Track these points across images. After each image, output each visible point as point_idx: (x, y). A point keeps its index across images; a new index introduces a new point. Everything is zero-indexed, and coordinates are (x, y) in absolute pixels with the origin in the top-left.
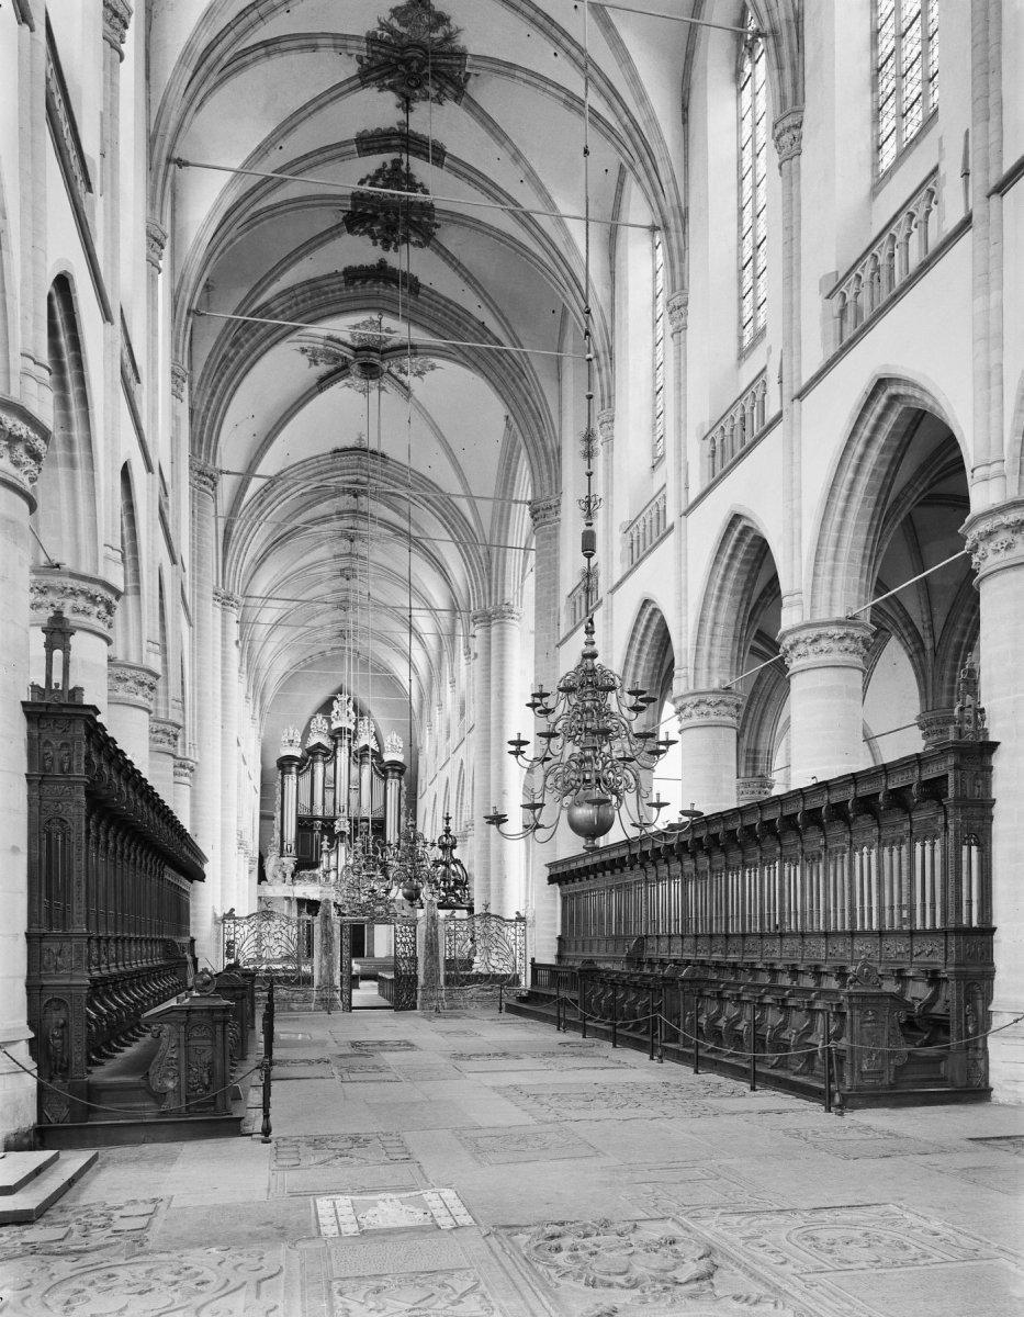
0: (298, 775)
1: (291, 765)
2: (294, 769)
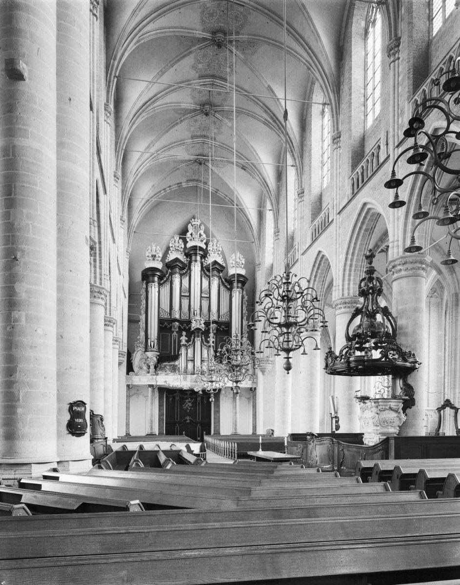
0: (160, 285)
1: (154, 275)
2: (156, 279)
